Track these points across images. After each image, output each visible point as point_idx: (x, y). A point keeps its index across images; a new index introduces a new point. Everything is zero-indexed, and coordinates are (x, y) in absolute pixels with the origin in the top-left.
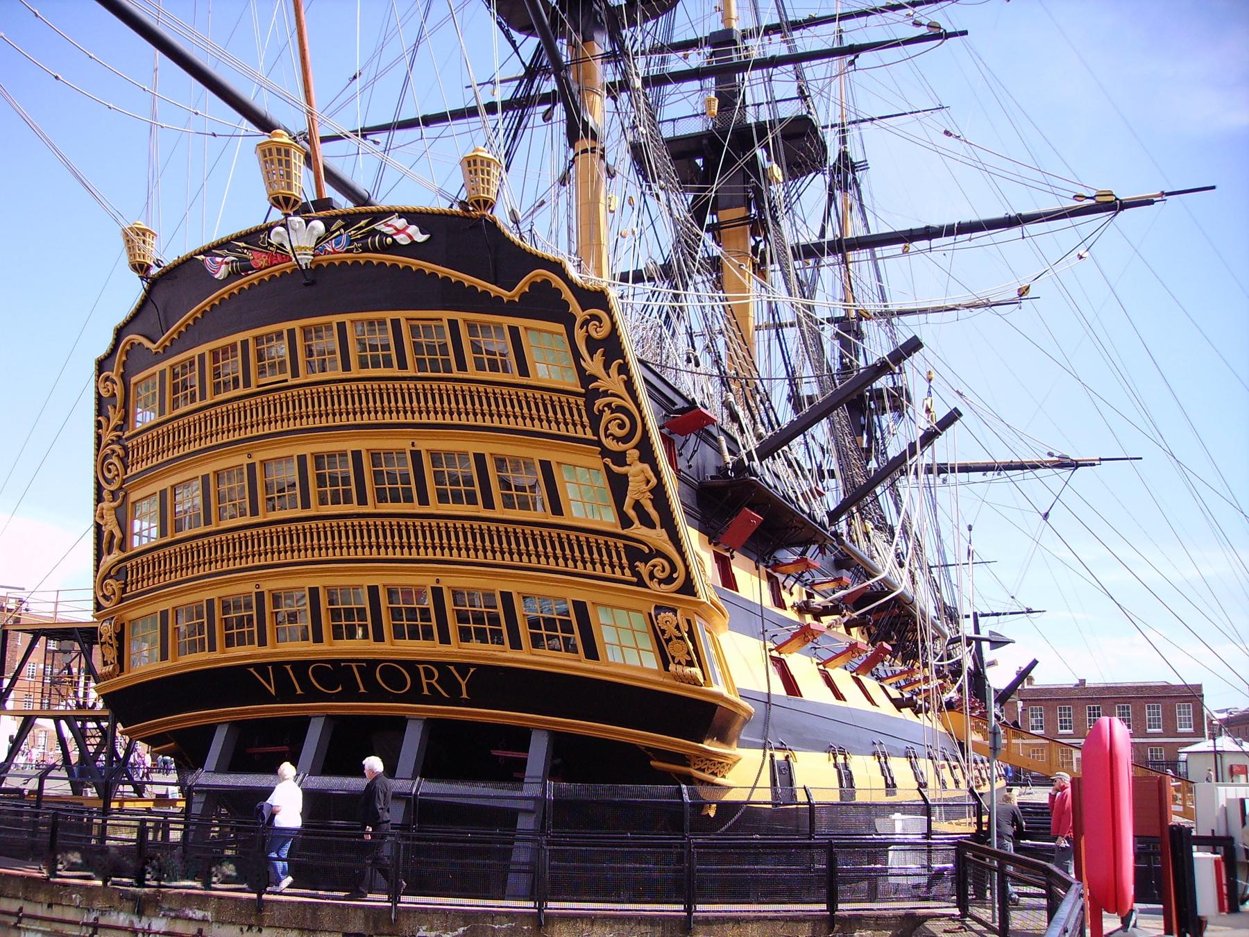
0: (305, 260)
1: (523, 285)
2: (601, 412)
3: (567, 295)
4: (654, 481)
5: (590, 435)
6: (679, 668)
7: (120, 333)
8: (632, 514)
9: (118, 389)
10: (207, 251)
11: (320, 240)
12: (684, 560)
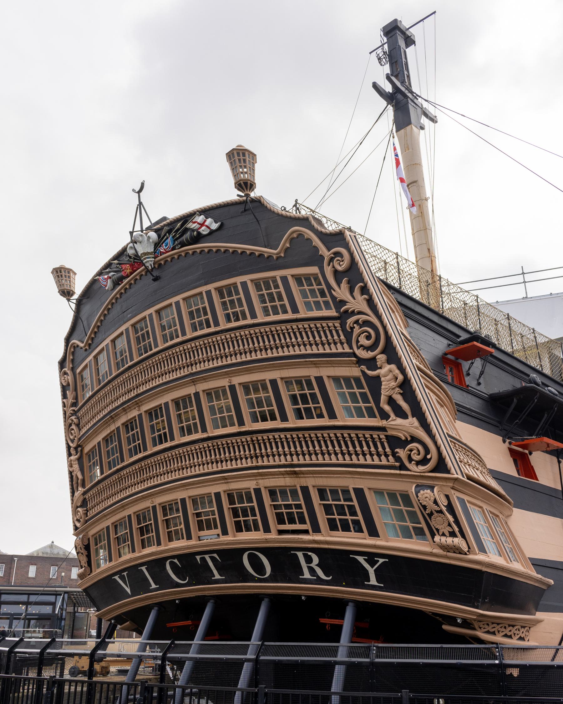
1: (284, 243)
2: (352, 328)
3: (317, 241)
4: (401, 377)
5: (347, 350)
6: (443, 539)
7: (68, 340)
8: (387, 408)
11: (157, 245)
12: (435, 443)
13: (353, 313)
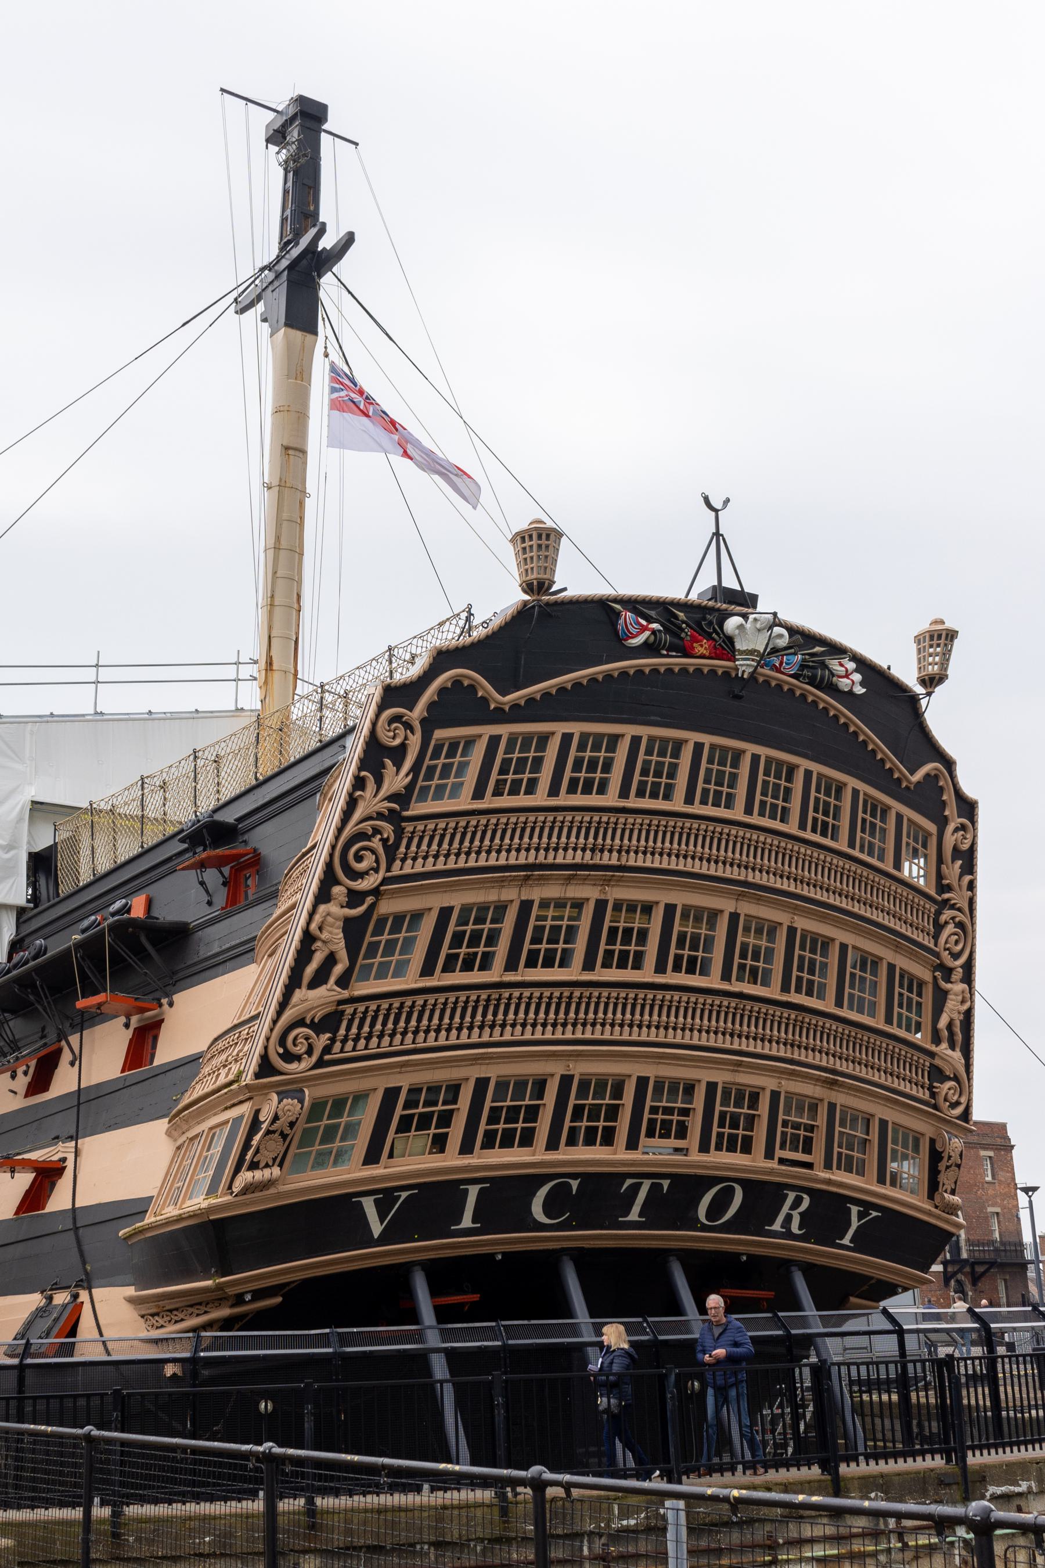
0: (745, 666)
2: (946, 923)
9: (415, 741)
10: (636, 605)
13: (953, 907)
